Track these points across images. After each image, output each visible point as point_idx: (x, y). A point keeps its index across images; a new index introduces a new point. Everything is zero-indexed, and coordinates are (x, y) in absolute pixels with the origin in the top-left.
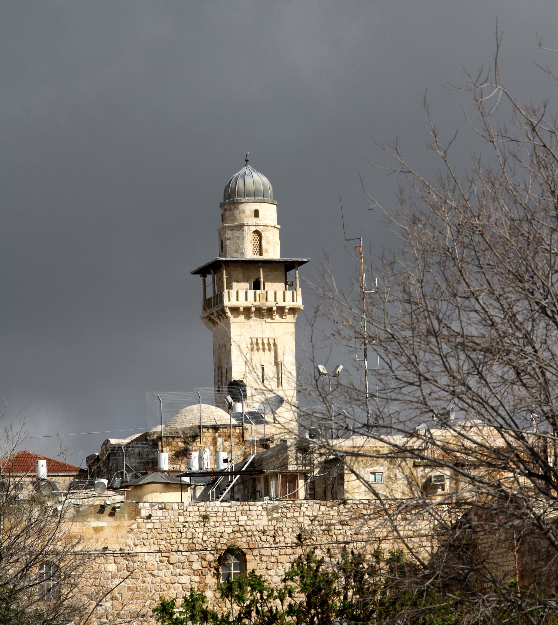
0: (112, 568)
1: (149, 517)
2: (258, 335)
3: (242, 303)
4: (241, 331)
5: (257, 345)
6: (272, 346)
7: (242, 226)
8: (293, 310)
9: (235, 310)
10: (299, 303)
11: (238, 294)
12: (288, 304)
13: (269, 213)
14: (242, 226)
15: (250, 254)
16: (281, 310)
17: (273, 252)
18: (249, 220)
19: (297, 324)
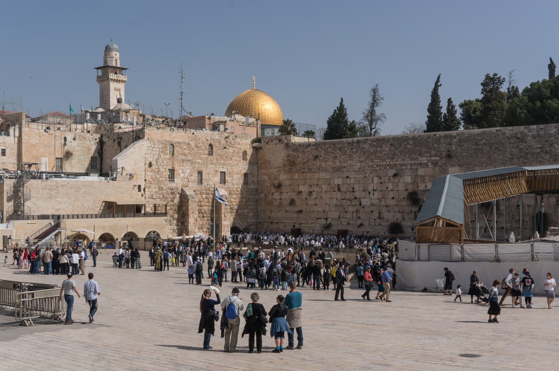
0: (185, 147)
1: (193, 134)
2: (116, 86)
3: (113, 78)
4: (113, 85)
5: (116, 89)
6: (119, 90)
7: (112, 57)
8: (125, 81)
9: (112, 79)
10: (126, 80)
11: (112, 76)
12: (124, 79)
13: (118, 54)
14: (112, 57)
15: (114, 65)
16: (122, 80)
17: (118, 66)
18: (114, 56)
19: (125, 85)
